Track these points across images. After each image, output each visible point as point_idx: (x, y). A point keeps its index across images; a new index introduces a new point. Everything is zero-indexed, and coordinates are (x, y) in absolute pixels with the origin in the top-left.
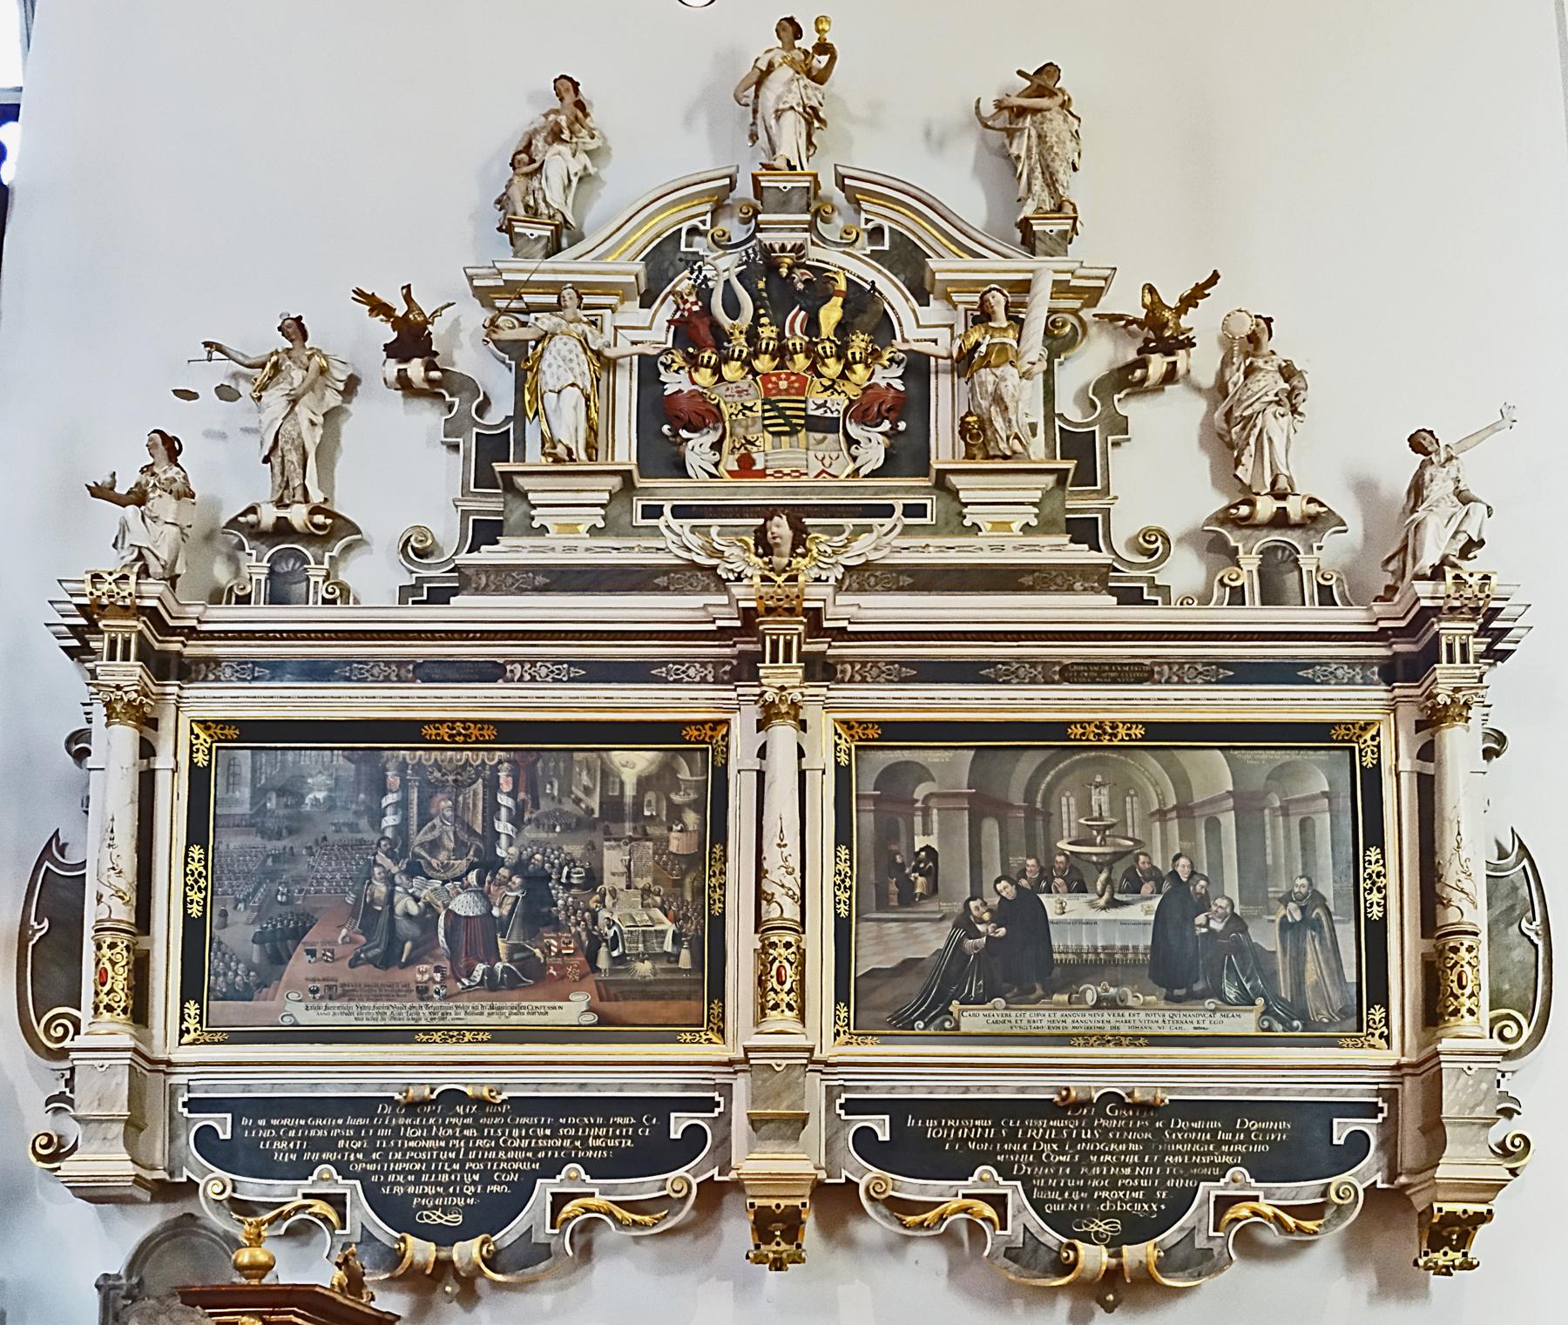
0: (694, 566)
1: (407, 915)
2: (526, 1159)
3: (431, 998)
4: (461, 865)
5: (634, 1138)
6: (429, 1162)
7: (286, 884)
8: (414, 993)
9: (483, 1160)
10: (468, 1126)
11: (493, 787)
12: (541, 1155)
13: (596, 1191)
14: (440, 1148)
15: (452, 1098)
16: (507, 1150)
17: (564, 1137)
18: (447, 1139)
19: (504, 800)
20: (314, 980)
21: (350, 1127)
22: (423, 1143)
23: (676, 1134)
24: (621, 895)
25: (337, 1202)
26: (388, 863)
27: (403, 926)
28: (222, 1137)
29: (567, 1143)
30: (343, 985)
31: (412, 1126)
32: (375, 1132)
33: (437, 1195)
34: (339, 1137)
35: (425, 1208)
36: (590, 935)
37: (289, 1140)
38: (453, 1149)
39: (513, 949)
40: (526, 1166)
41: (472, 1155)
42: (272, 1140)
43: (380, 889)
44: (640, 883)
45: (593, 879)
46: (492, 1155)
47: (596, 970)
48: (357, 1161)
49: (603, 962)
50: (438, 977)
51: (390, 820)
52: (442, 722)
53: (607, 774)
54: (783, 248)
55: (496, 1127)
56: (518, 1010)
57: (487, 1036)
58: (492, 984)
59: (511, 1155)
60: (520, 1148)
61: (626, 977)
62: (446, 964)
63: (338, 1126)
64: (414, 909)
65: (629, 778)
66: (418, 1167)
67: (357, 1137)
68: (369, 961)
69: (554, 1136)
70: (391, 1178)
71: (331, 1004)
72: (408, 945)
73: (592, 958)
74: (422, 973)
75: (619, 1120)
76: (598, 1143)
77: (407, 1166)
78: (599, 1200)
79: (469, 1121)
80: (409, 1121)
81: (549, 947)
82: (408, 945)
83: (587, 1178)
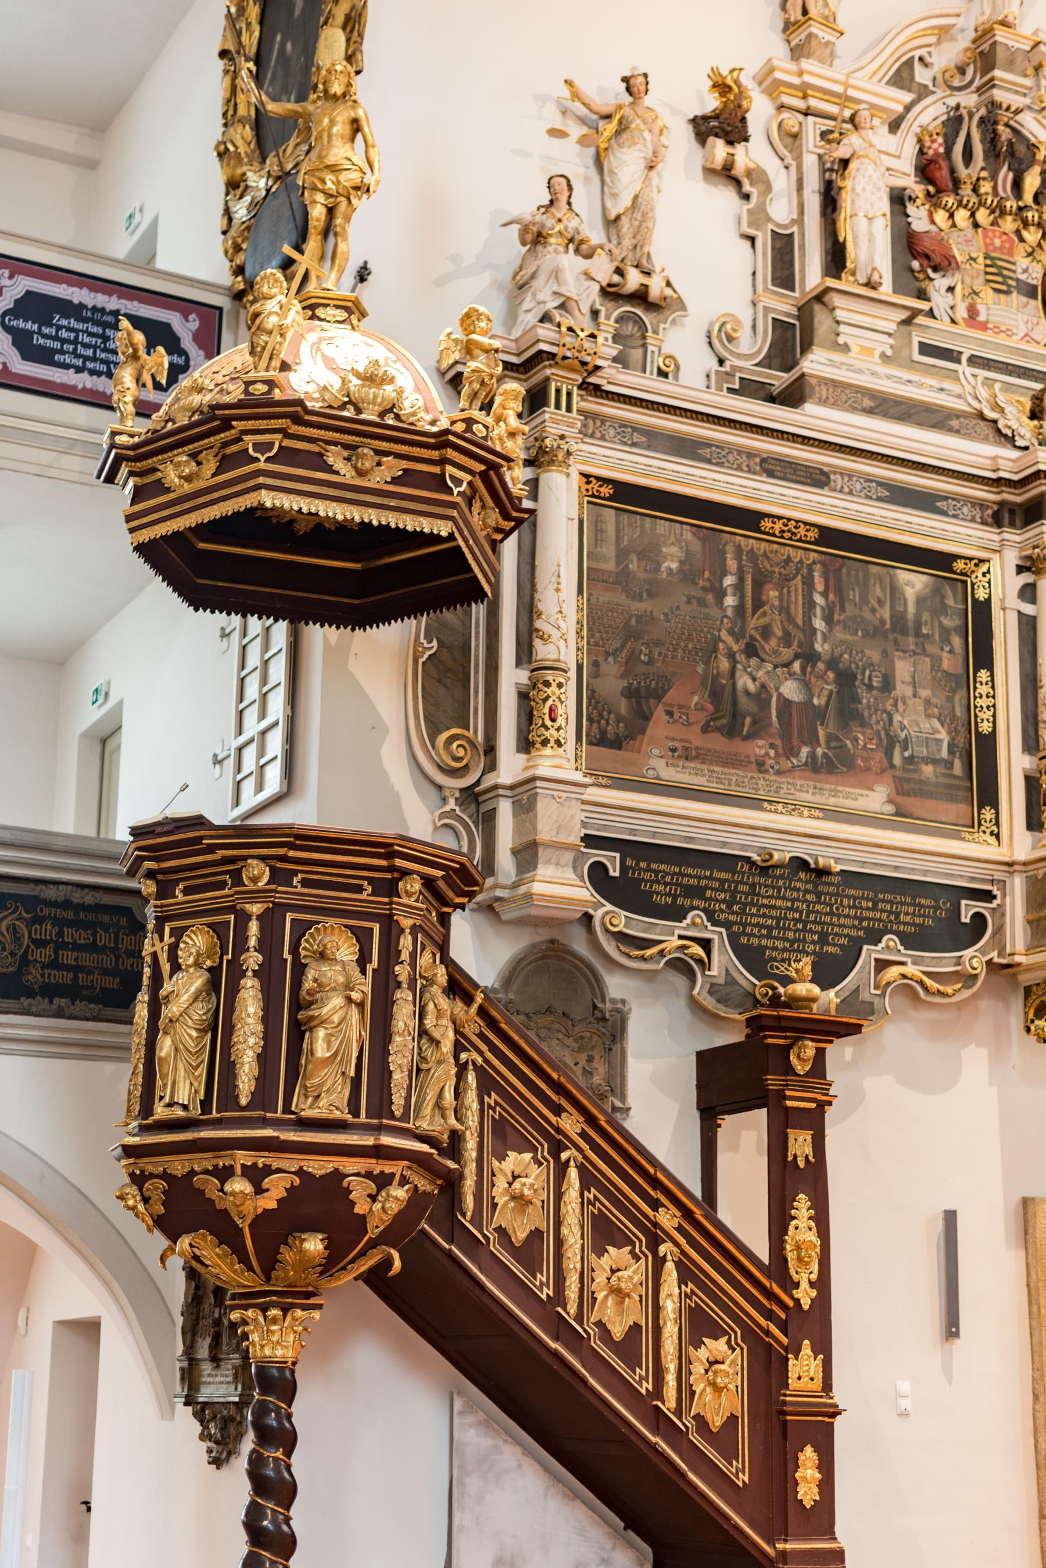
0: (981, 416)
1: (747, 692)
2: (854, 927)
3: (766, 772)
4: (787, 653)
5: (936, 919)
6: (778, 919)
7: (648, 646)
8: (754, 766)
9: (820, 923)
10: (807, 891)
11: (809, 584)
12: (865, 924)
13: (909, 960)
14: (787, 909)
15: (800, 864)
16: (839, 916)
17: (882, 911)
18: (793, 900)
19: (819, 599)
20: (673, 739)
21: (716, 879)
22: (773, 902)
23: (966, 919)
24: (909, 702)
26: (730, 640)
27: (743, 700)
28: (612, 873)
29: (884, 916)
30: (697, 748)
31: (766, 886)
32: (736, 887)
33: (784, 950)
34: (706, 888)
35: (775, 959)
36: (887, 735)
37: (666, 884)
38: (796, 910)
39: (830, 738)
40: (853, 933)
41: (812, 917)
42: (653, 882)
43: (724, 664)
44: (925, 693)
45: (888, 684)
46: (828, 919)
47: (892, 766)
48: (722, 911)
49: (897, 760)
50: (772, 753)
51: (730, 601)
52: (780, 518)
53: (895, 591)
54: (1008, 109)
55: (831, 895)
56: (835, 793)
57: (817, 813)
58: (814, 766)
59: (842, 920)
60: (848, 916)
61: (915, 776)
62: (778, 742)
63: (706, 877)
64: (752, 687)
65: (910, 594)
66: (769, 922)
67: (723, 890)
68: (719, 729)
69: (874, 908)
70: (748, 930)
71: (687, 764)
72: (748, 720)
73: (889, 754)
74: (759, 748)
75: (923, 901)
76: (908, 919)
77: (762, 921)
78: (911, 970)
79: (809, 886)
80: (762, 880)
81: (857, 740)
82: (748, 720)
83: (901, 948)
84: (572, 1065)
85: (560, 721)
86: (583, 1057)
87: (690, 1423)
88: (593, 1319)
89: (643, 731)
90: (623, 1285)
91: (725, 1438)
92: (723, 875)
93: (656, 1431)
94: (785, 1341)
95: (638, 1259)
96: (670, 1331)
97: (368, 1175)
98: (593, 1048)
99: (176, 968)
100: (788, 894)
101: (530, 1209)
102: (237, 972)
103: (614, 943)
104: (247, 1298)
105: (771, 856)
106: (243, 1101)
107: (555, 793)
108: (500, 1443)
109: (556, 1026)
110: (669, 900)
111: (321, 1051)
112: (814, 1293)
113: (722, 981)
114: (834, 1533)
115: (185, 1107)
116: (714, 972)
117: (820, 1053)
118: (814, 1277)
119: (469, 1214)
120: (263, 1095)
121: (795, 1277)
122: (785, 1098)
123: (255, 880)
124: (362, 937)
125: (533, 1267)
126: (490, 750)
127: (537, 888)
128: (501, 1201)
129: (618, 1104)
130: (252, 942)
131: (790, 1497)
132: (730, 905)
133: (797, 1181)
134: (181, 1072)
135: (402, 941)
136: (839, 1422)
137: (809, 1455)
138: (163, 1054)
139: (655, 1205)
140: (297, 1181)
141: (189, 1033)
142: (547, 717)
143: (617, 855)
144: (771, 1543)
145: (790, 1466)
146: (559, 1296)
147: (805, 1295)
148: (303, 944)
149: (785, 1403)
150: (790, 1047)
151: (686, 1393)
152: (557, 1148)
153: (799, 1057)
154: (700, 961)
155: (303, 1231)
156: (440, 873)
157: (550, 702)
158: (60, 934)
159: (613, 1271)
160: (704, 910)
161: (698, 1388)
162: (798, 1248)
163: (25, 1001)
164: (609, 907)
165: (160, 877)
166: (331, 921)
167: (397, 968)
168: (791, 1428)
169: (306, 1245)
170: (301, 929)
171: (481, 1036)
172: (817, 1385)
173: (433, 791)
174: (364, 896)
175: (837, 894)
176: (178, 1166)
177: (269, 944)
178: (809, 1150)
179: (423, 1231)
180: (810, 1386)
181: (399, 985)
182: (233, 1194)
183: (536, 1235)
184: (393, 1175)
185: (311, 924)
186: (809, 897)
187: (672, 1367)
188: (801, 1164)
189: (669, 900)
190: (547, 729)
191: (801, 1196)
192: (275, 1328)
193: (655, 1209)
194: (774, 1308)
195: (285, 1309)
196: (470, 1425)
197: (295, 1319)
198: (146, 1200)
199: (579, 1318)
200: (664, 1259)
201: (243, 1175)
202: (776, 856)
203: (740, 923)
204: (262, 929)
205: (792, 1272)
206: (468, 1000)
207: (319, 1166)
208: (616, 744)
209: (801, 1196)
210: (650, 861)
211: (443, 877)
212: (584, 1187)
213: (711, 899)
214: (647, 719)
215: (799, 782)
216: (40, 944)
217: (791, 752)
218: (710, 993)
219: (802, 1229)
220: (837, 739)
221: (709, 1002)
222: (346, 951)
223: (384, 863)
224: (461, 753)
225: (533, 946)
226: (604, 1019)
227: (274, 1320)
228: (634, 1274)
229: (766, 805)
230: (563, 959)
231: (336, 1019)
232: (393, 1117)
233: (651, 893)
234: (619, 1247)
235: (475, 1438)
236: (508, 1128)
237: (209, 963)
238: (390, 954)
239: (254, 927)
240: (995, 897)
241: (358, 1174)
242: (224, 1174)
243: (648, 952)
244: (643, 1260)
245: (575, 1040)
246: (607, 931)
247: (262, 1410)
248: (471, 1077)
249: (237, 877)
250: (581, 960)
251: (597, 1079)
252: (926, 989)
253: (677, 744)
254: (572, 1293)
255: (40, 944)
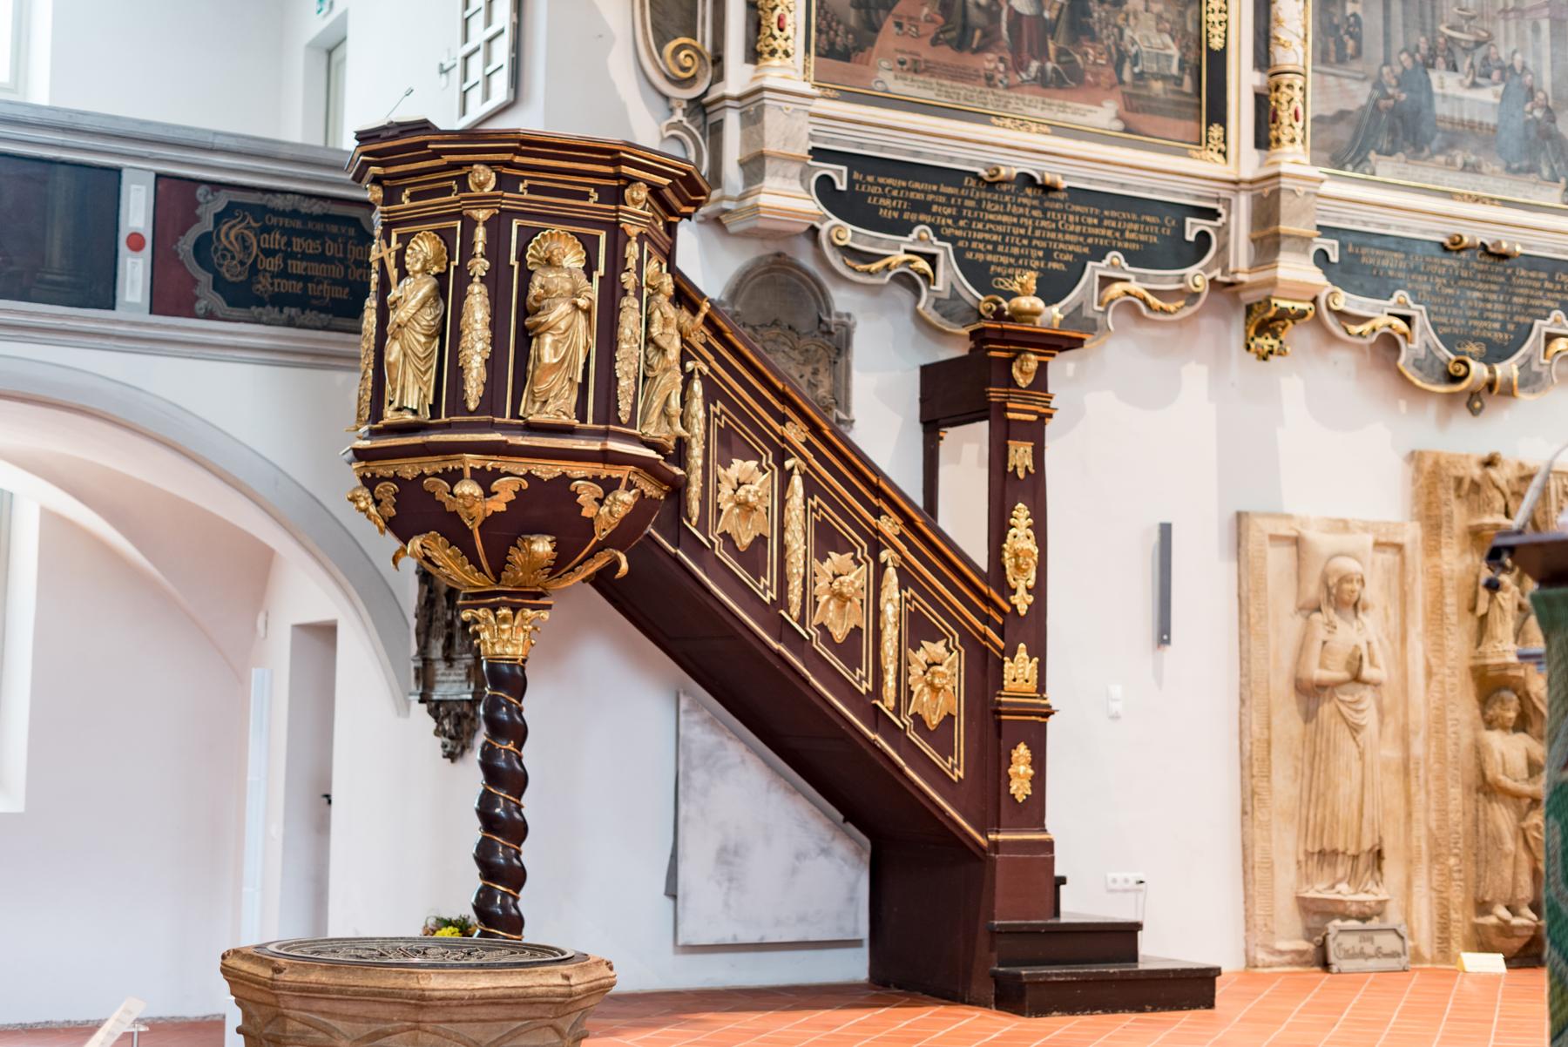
2: (1079, 243)
3: (995, 86)
5: (1160, 236)
6: (1004, 235)
8: (983, 80)
9: (1046, 239)
10: (1033, 207)
12: (1090, 240)
13: (1132, 277)
14: (1013, 224)
15: (1027, 180)
16: (1064, 232)
17: (1107, 228)
18: (1019, 216)
20: (902, 52)
22: (999, 218)
23: (1190, 236)
24: (1141, 17)
25: (931, 259)
29: (1109, 233)
30: (926, 61)
33: (1010, 265)
34: (933, 202)
35: (999, 275)
36: (1118, 50)
37: (893, 198)
38: (1022, 226)
39: (1060, 52)
40: (1078, 249)
41: (1038, 233)
42: (879, 196)
44: (1157, 7)
46: (1053, 235)
47: (1122, 82)
48: (948, 226)
49: (1127, 76)
56: (1063, 109)
57: (1046, 129)
59: (1068, 237)
60: (1073, 233)
61: (1144, 92)
62: (1008, 56)
63: (933, 192)
66: (995, 238)
67: (949, 205)
68: (948, 42)
69: (1100, 226)
71: (916, 77)
72: (978, 34)
73: (1119, 69)
74: (989, 62)
75: (1148, 219)
76: (1133, 236)
77: (987, 236)
78: (1135, 287)
79: (1036, 203)
80: (989, 196)
81: (1086, 54)
82: (978, 34)
84: (797, 376)
85: (789, 31)
86: (808, 370)
87: (908, 721)
88: (815, 621)
89: (872, 43)
90: (845, 590)
91: (941, 736)
92: (950, 190)
93: (875, 729)
94: (1001, 644)
95: (859, 564)
96: (890, 634)
97: (595, 479)
98: (818, 361)
99: (404, 274)
100: (1014, 210)
101: (755, 515)
102: (464, 278)
103: (840, 257)
104: (477, 599)
105: (998, 171)
106: (472, 406)
107: (783, 105)
108: (725, 740)
109: (782, 339)
110: (896, 215)
111: (548, 357)
112: (1031, 599)
113: (946, 295)
114: (1043, 825)
115: (415, 412)
116: (939, 286)
117: (1042, 367)
118: (1031, 583)
119: (695, 520)
120: (491, 399)
121: (1013, 583)
122: (1007, 410)
123: (481, 185)
124: (589, 245)
125: (757, 571)
126: (718, 60)
127: (764, 200)
128: (726, 507)
129: (842, 416)
130: (479, 248)
131: (1003, 791)
132: (956, 219)
133: (1016, 491)
134: (410, 377)
135: (628, 249)
136: (1051, 722)
137: (1022, 752)
138: (392, 359)
139: (877, 513)
140: (525, 485)
141: (416, 338)
142: (775, 27)
143: (845, 169)
144: (984, 834)
145: (1004, 762)
146: (782, 601)
147: (1022, 601)
148: (530, 251)
149: (1000, 703)
150: (1013, 360)
151: (905, 693)
152: (781, 456)
153: (1021, 370)
154: (925, 276)
155: (532, 534)
156: (667, 181)
157: (778, 12)
158: (289, 244)
159: (835, 576)
160: (931, 225)
161: (916, 689)
162: (1016, 556)
163: (255, 310)
164: (836, 220)
165: (386, 183)
166: (557, 228)
167: (623, 276)
168: (1005, 726)
169: (535, 547)
170: (527, 235)
171: (708, 345)
172: (1032, 685)
173: (660, 101)
174: (590, 203)
175: (1063, 211)
176: (409, 469)
177: (496, 250)
178: (1029, 462)
179: (649, 536)
180: (1026, 687)
181: (625, 293)
182: (463, 496)
183: (761, 540)
184: (620, 479)
185: (537, 231)
186: (1036, 213)
187: (890, 668)
188: (1021, 475)
189: (896, 215)
190: (775, 38)
191: (1020, 505)
192: (505, 626)
193: (877, 517)
194: (992, 613)
195: (515, 609)
196: (696, 723)
197: (524, 619)
198: (377, 502)
199: (802, 621)
200: (885, 565)
201: (473, 478)
202: (1003, 172)
203: (966, 239)
204: (489, 235)
205: (1010, 579)
206: (694, 309)
207: (547, 470)
208: (845, 56)
209: (1020, 505)
210: (876, 174)
211: (669, 185)
212: (808, 494)
213: (937, 214)
214: (876, 30)
215: (1028, 97)
216: (269, 253)
217: (1020, 66)
218: (935, 307)
219: (1020, 536)
220: (1068, 54)
221: (934, 317)
222: (573, 259)
223: (610, 170)
224: (688, 63)
225: (760, 259)
226: (830, 333)
227: (504, 620)
228: (856, 578)
229: (994, 120)
230: (789, 272)
231: (563, 325)
232: (620, 423)
233: (877, 208)
234: (842, 553)
235: (700, 735)
236: (733, 437)
237: (436, 269)
238: (616, 261)
239: (480, 234)
240: (1220, 215)
241: (585, 479)
242: (454, 477)
243: (874, 267)
244: (864, 567)
245: (801, 353)
246: (833, 244)
247: (494, 705)
248: (697, 386)
249: (463, 182)
250: (808, 274)
251: (821, 392)
252: (1148, 306)
253: (906, 57)
254: (795, 596)
255: (269, 253)
